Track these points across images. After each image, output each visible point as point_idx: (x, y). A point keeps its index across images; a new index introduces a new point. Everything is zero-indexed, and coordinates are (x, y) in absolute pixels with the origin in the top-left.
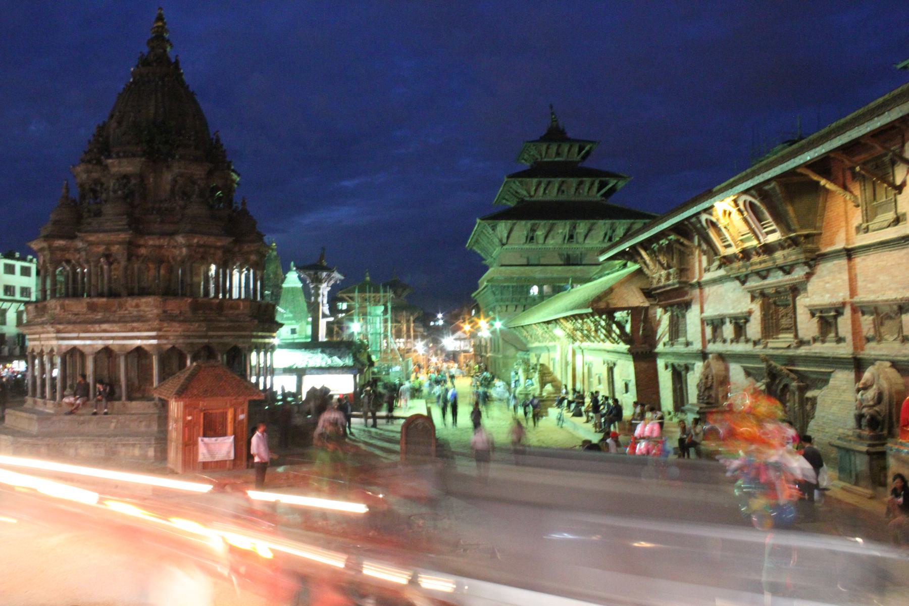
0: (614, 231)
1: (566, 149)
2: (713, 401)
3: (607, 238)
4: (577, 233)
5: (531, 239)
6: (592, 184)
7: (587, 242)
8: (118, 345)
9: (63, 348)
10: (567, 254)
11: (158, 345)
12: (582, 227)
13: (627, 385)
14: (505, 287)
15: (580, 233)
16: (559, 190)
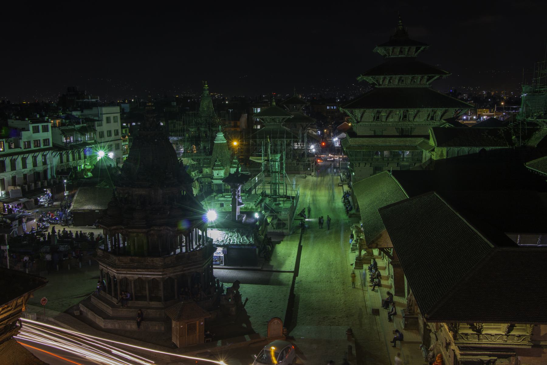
0: (435, 113)
1: (407, 50)
2: (412, 312)
3: (430, 118)
4: (409, 114)
5: (377, 118)
6: (422, 77)
7: (415, 120)
8: (146, 277)
9: (120, 277)
10: (401, 128)
11: (163, 278)
12: (412, 112)
13: (392, 276)
14: (358, 151)
15: (412, 114)
16: (399, 80)
